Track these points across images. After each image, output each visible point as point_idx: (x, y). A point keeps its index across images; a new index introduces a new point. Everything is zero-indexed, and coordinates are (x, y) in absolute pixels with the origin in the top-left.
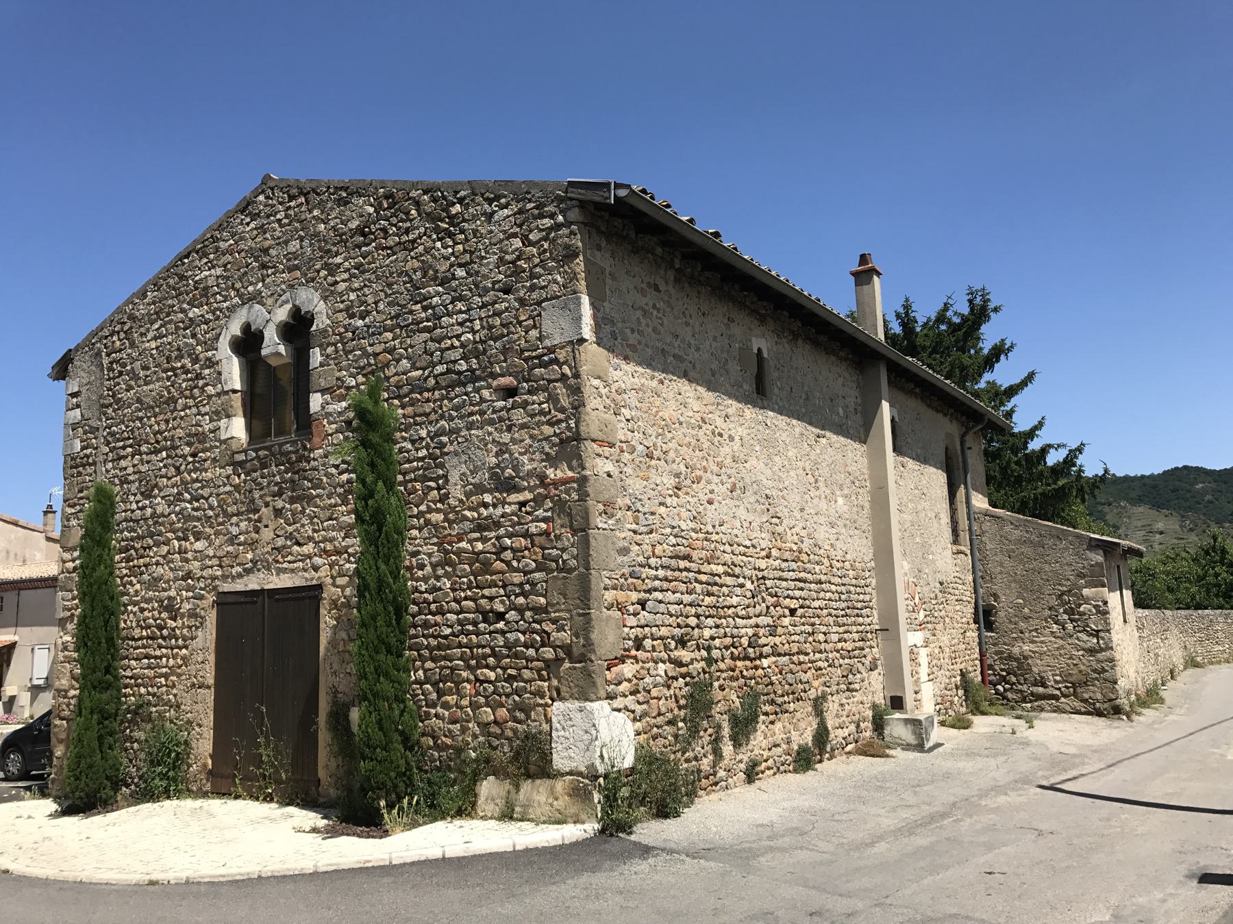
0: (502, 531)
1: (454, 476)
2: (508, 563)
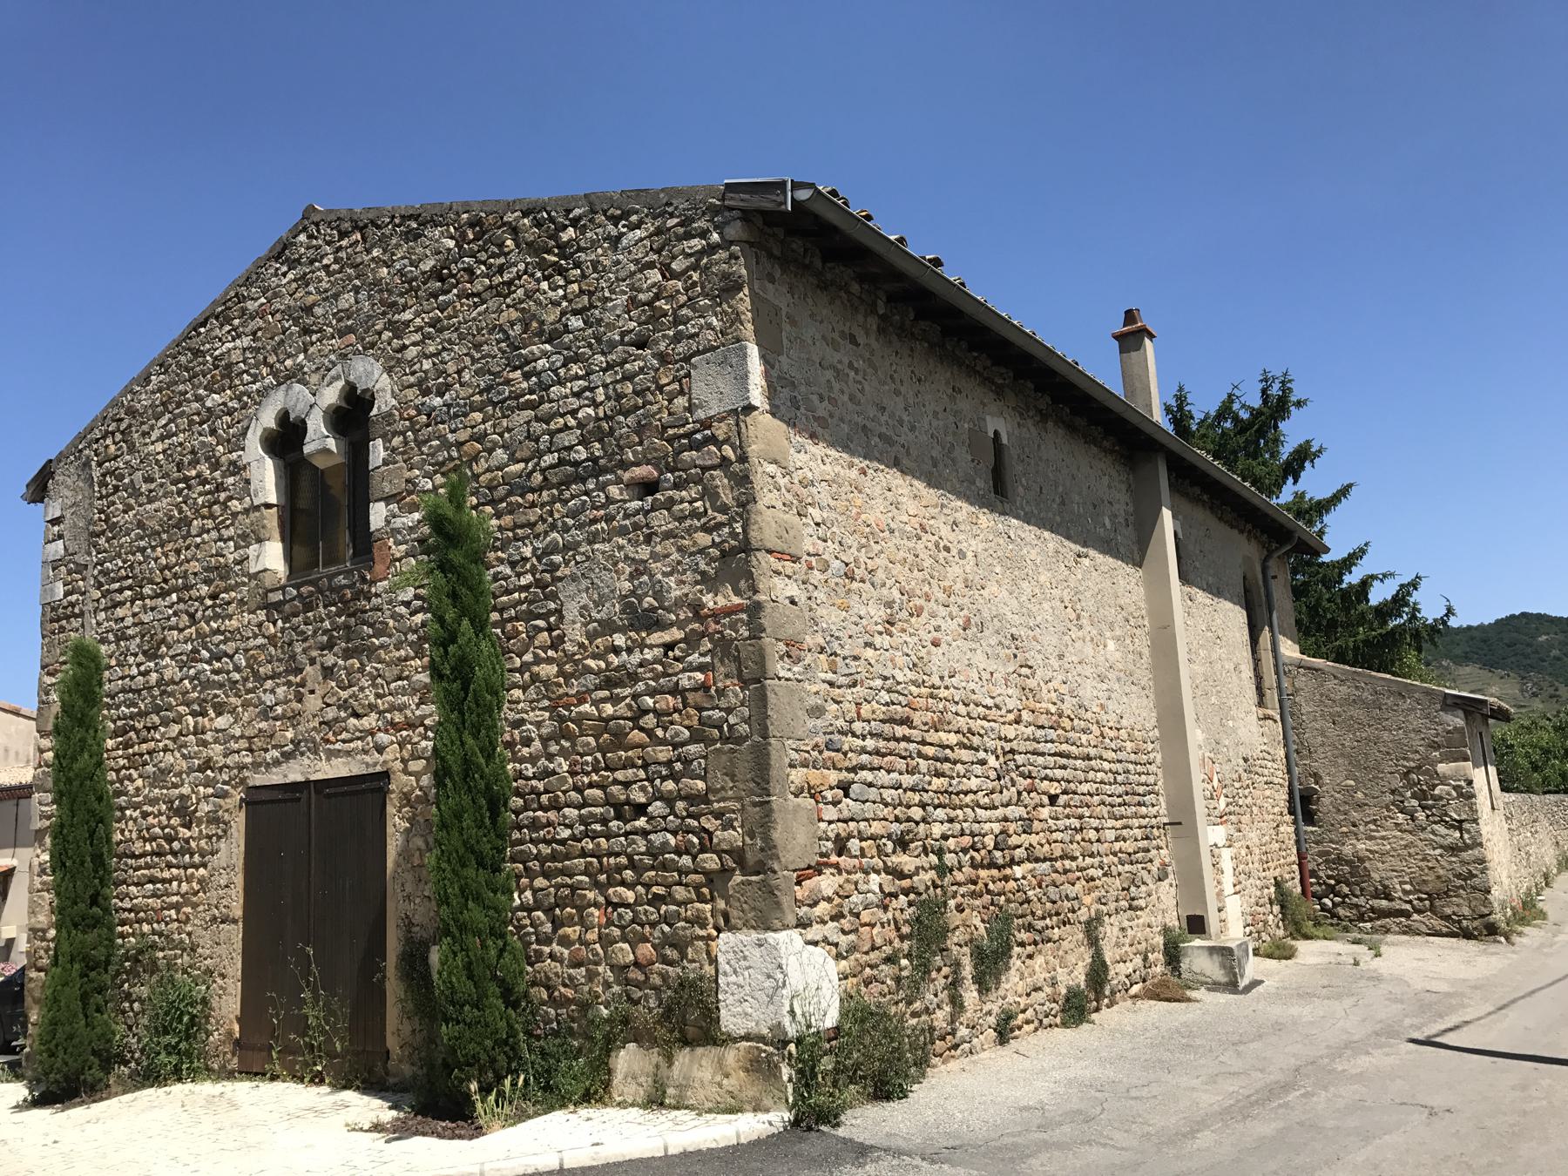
0: (640, 686)
1: (571, 611)
2: (650, 733)
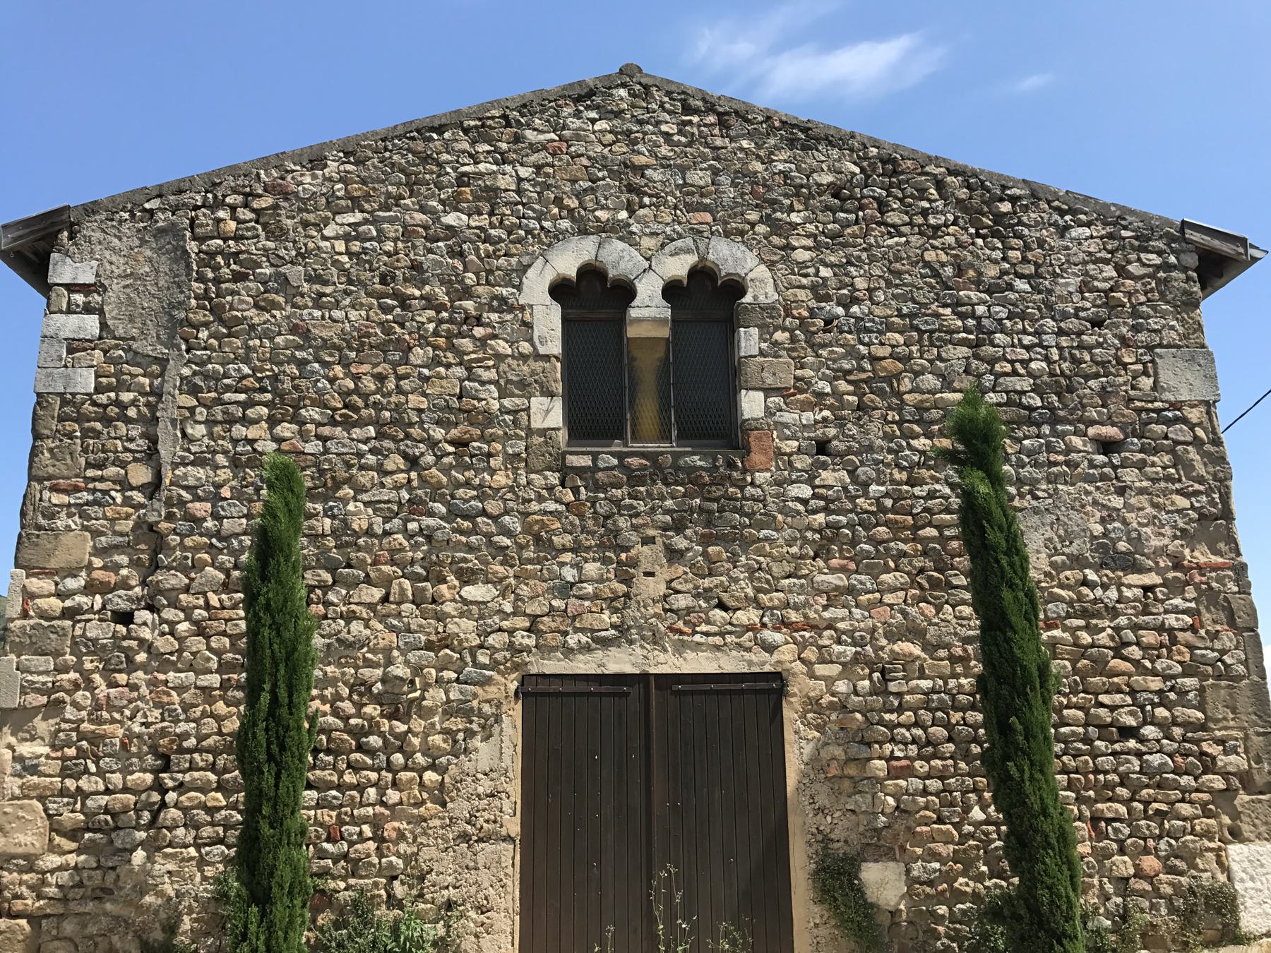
0: (1122, 621)
2: (1137, 663)
